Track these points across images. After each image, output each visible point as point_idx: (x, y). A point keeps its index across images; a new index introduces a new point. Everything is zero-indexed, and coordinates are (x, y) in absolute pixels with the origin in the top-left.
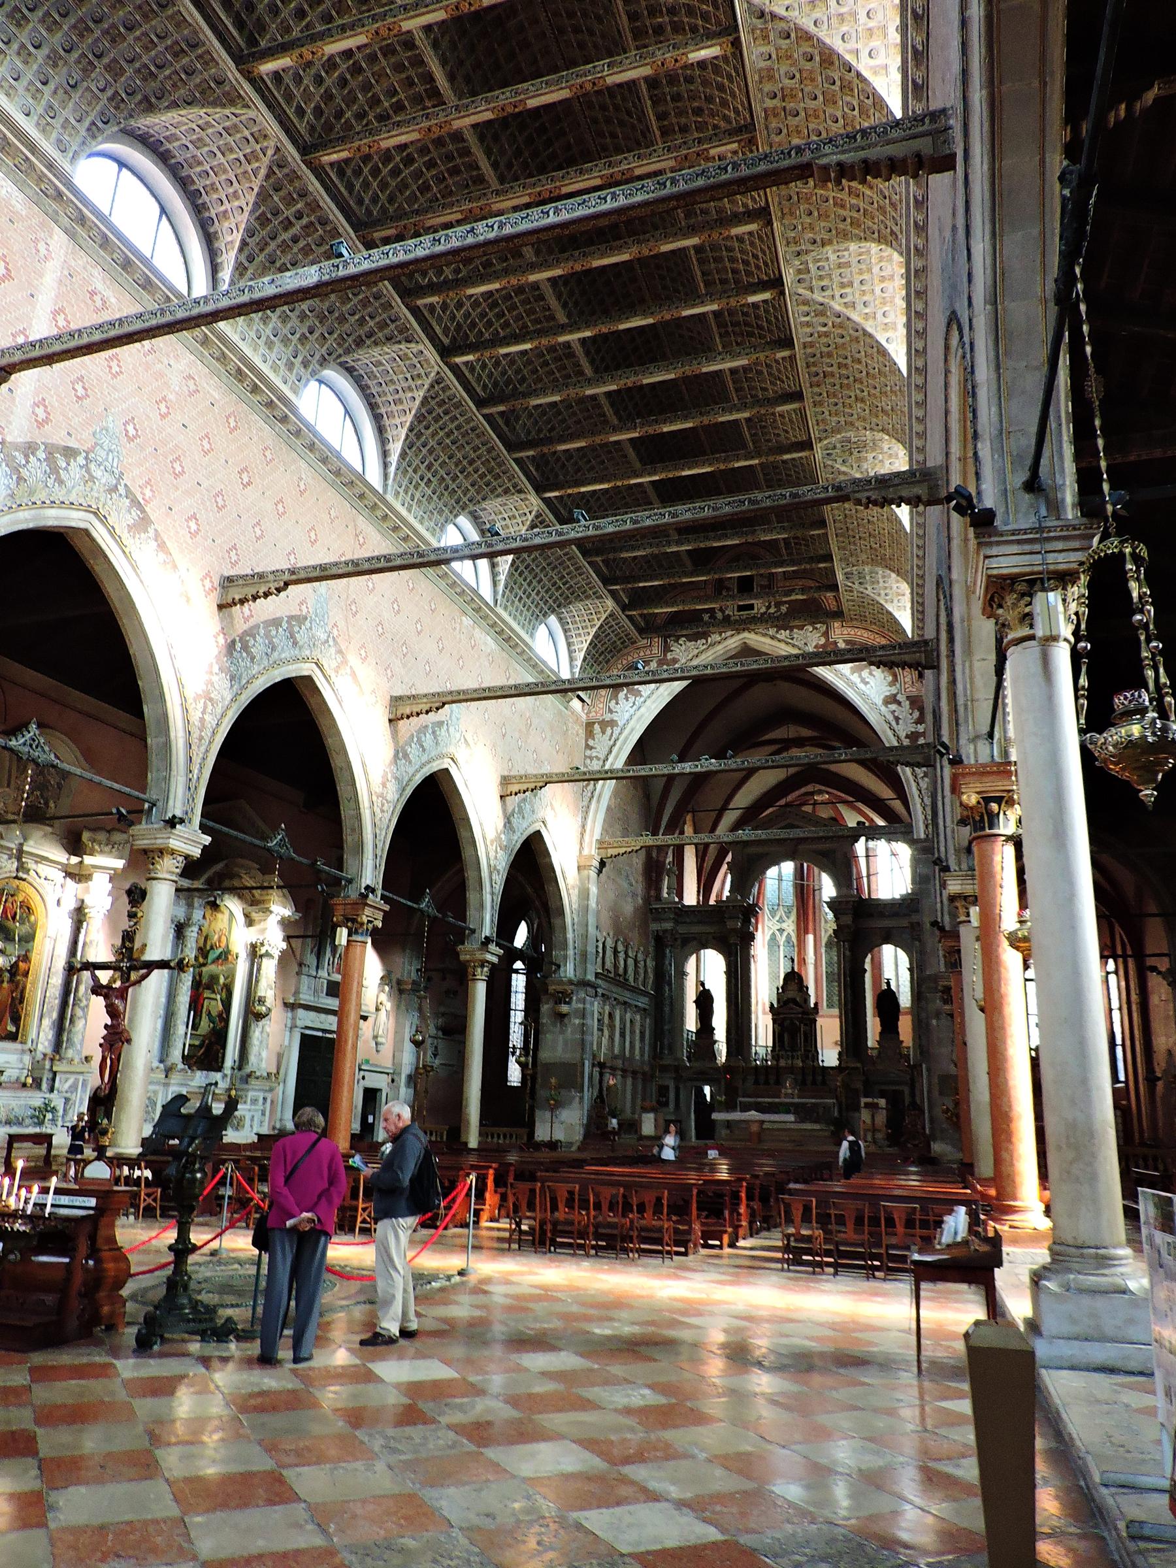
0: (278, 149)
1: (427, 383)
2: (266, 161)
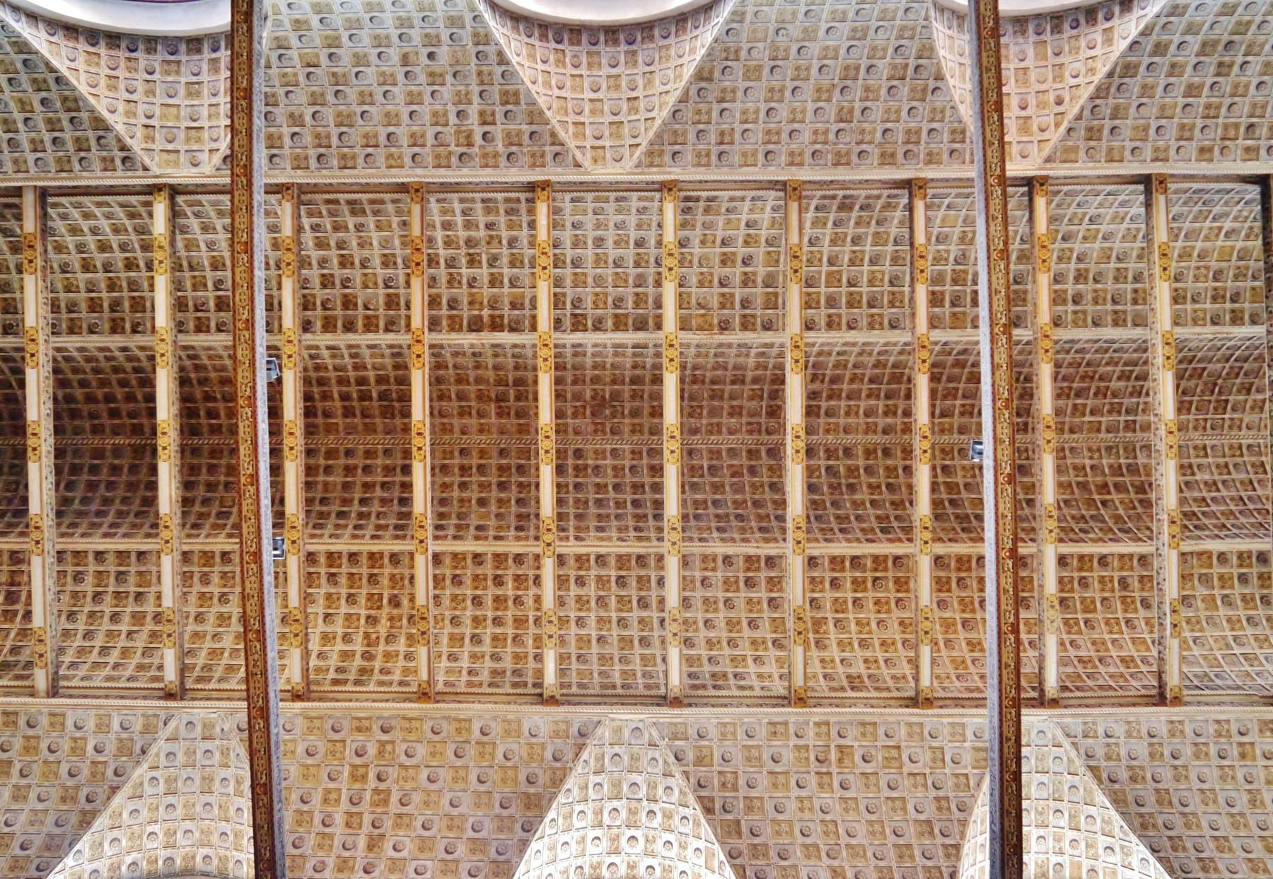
0: (578, 165)
1: (136, 145)
2: (571, 144)
